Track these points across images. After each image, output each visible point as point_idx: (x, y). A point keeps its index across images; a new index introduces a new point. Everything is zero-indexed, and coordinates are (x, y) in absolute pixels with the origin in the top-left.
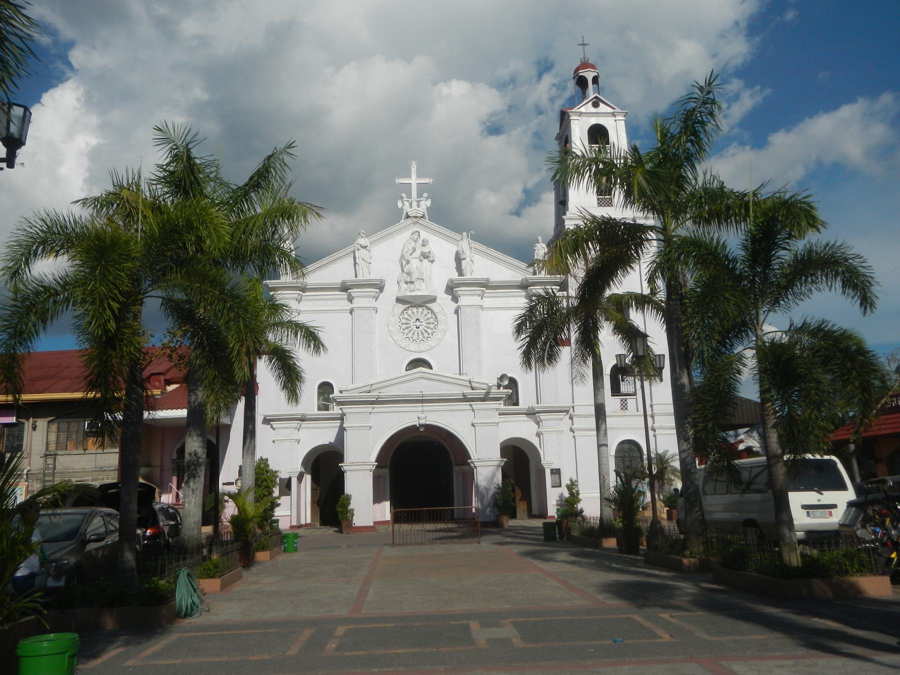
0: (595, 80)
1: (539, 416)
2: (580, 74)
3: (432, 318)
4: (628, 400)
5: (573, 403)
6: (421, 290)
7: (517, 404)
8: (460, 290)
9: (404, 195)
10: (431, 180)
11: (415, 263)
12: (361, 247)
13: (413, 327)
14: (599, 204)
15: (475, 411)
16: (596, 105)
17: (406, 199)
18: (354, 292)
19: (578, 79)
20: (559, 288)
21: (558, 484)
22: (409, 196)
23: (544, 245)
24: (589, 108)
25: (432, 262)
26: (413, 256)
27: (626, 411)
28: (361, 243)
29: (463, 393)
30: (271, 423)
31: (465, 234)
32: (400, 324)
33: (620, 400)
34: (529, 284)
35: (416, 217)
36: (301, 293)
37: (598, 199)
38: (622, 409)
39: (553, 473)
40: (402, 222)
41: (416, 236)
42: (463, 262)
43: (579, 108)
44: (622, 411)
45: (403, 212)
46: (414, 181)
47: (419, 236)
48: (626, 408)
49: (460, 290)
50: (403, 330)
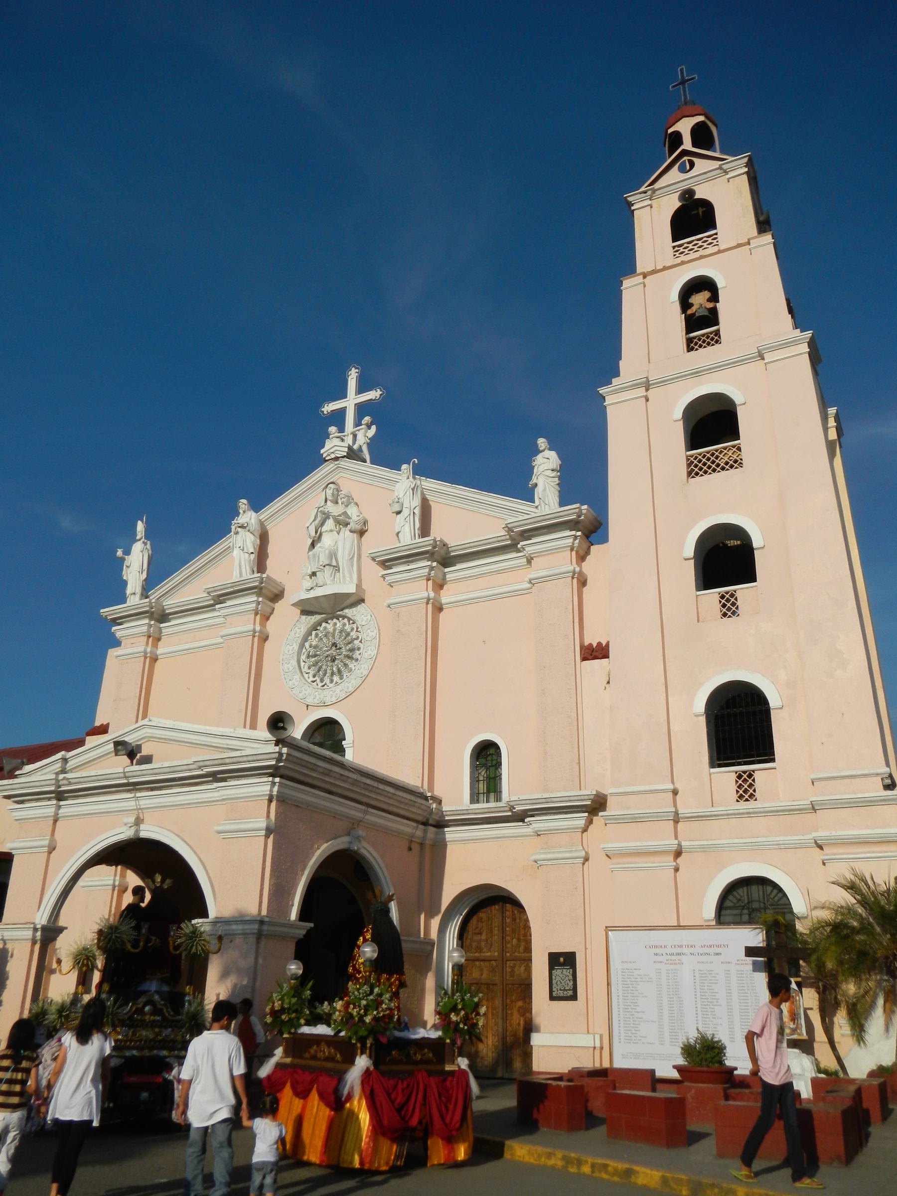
2: (670, 131)
4: (756, 775)
6: (330, 586)
7: (498, 799)
9: (333, 429)
10: (379, 392)
11: (327, 541)
12: (239, 527)
21: (570, 993)
23: (553, 455)
25: (361, 533)
26: (324, 528)
27: (752, 801)
32: (303, 657)
33: (734, 776)
35: (336, 459)
36: (152, 622)
37: (689, 341)
38: (741, 797)
39: (563, 964)
41: (329, 492)
44: (742, 802)
47: (338, 490)
48: (751, 796)
50: (309, 668)
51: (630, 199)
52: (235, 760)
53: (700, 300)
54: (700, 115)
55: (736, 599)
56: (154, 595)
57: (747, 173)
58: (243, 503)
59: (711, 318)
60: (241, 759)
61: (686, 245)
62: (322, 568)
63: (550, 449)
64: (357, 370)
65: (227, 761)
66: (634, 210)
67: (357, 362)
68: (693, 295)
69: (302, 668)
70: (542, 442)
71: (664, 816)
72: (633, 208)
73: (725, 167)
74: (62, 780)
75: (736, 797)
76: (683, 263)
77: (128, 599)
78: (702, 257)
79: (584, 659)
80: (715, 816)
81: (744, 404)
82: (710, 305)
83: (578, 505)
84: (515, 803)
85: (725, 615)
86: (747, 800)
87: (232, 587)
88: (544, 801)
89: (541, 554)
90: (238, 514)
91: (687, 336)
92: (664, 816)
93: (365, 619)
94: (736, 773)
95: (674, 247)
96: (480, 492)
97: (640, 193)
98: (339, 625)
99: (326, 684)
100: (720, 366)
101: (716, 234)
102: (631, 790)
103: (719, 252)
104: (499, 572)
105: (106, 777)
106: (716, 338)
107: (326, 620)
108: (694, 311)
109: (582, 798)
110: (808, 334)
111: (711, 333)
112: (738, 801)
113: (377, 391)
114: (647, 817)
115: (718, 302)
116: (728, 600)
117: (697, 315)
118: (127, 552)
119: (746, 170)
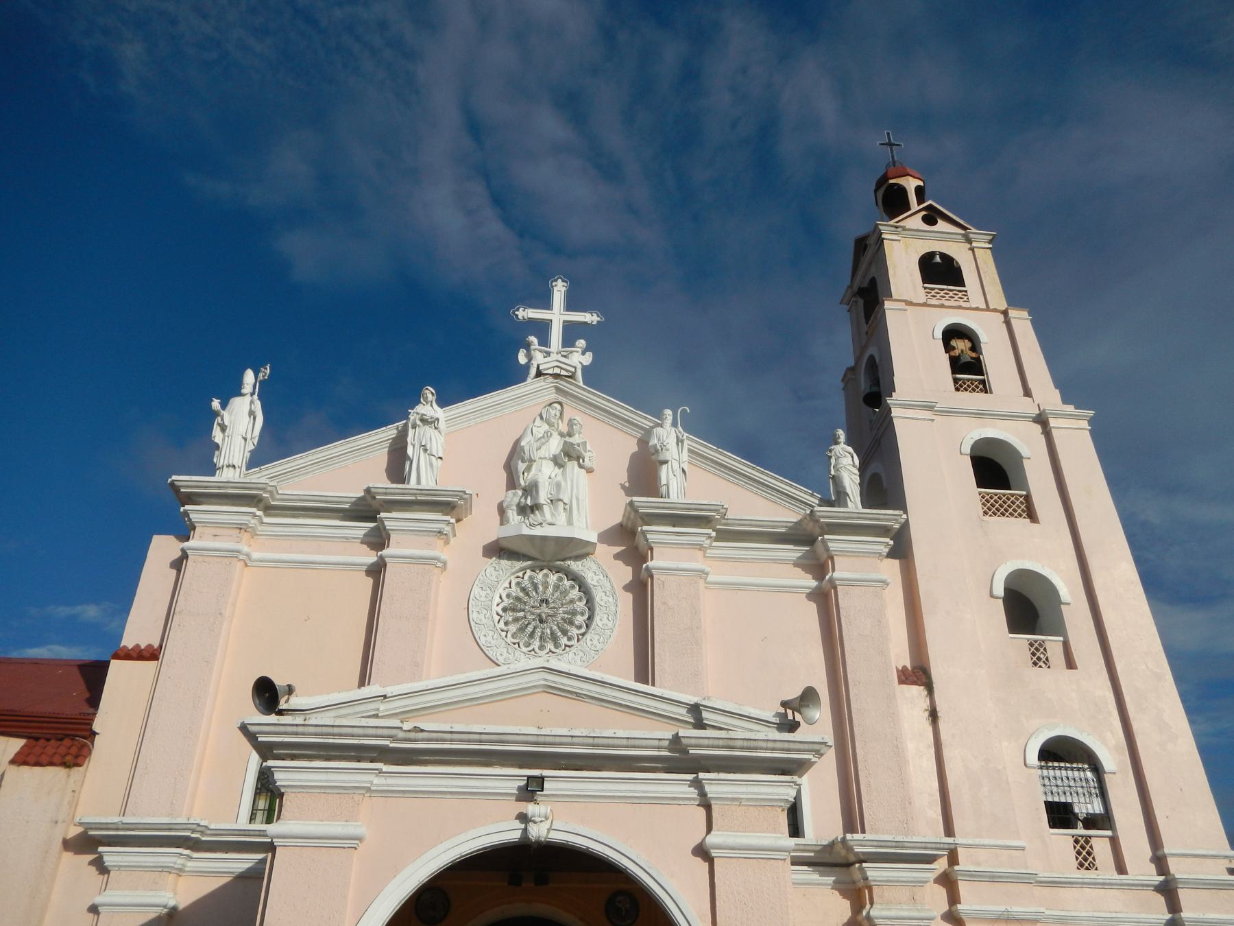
0: (920, 191)
1: (862, 870)
2: (892, 181)
3: (580, 599)
4: (1093, 841)
5: (949, 831)
8: (656, 534)
9: (533, 339)
12: (422, 420)
13: (530, 617)
14: (957, 389)
15: (713, 802)
16: (930, 219)
17: (537, 347)
18: (391, 520)
19: (885, 191)
20: (892, 542)
22: (545, 341)
23: (850, 449)
24: (916, 222)
27: (1093, 871)
28: (423, 412)
29: (676, 739)
30: (101, 849)
31: (668, 412)
32: (499, 609)
33: (1071, 840)
34: (817, 530)
35: (556, 376)
36: (259, 513)
37: (956, 381)
40: (529, 380)
42: (664, 472)
43: (897, 222)
44: (1082, 870)
45: (528, 373)
46: (557, 315)
47: (562, 413)
49: (656, 534)
50: (506, 624)
51: (881, 227)
52: (753, 744)
53: (961, 345)
54: (920, 179)
55: (1045, 649)
56: (260, 476)
57: (990, 248)
58: (429, 393)
59: (975, 367)
60: (763, 744)
61: (936, 291)
62: (550, 502)
63: (848, 443)
64: (565, 284)
65: (739, 743)
66: (884, 239)
67: (567, 277)
68: (954, 339)
69: (496, 624)
70: (841, 435)
71: (1025, 878)
72: (883, 236)
73: (971, 236)
74: (409, 731)
75: (1076, 864)
76: (942, 306)
77: (218, 472)
78: (960, 307)
79: (901, 682)
80: (1070, 883)
81: (1029, 458)
82: (974, 355)
83: (901, 512)
84: (856, 843)
85: (1035, 664)
86: (1087, 869)
87: (415, 494)
88: (894, 844)
89: (845, 553)
90: (419, 402)
91: (954, 375)
92: (1025, 878)
93: (596, 578)
94: (1073, 837)
95: (925, 288)
96: (755, 466)
97: (892, 226)
98: (553, 578)
99: (533, 650)
100: (1004, 416)
101: (966, 292)
102: (982, 843)
103: (977, 309)
104: (775, 561)
105: (501, 738)
106: (985, 387)
107: (534, 567)
108: (957, 354)
109: (938, 846)
110: (1091, 413)
111: (976, 380)
112: (1079, 869)
113: (592, 316)
114: (1007, 877)
115: (982, 354)
116: (1037, 649)
117: (963, 360)
118: (224, 405)
119: (991, 246)
